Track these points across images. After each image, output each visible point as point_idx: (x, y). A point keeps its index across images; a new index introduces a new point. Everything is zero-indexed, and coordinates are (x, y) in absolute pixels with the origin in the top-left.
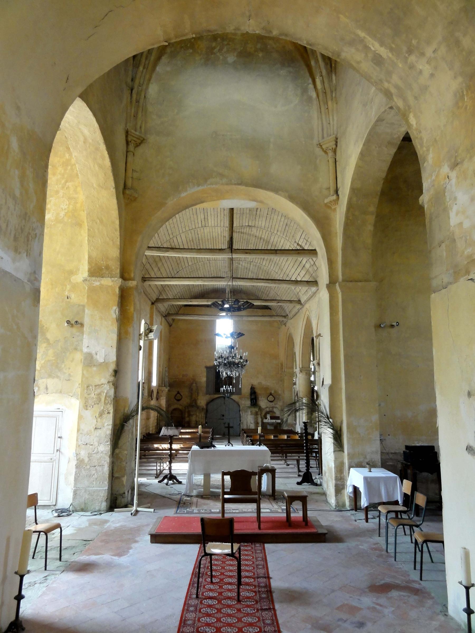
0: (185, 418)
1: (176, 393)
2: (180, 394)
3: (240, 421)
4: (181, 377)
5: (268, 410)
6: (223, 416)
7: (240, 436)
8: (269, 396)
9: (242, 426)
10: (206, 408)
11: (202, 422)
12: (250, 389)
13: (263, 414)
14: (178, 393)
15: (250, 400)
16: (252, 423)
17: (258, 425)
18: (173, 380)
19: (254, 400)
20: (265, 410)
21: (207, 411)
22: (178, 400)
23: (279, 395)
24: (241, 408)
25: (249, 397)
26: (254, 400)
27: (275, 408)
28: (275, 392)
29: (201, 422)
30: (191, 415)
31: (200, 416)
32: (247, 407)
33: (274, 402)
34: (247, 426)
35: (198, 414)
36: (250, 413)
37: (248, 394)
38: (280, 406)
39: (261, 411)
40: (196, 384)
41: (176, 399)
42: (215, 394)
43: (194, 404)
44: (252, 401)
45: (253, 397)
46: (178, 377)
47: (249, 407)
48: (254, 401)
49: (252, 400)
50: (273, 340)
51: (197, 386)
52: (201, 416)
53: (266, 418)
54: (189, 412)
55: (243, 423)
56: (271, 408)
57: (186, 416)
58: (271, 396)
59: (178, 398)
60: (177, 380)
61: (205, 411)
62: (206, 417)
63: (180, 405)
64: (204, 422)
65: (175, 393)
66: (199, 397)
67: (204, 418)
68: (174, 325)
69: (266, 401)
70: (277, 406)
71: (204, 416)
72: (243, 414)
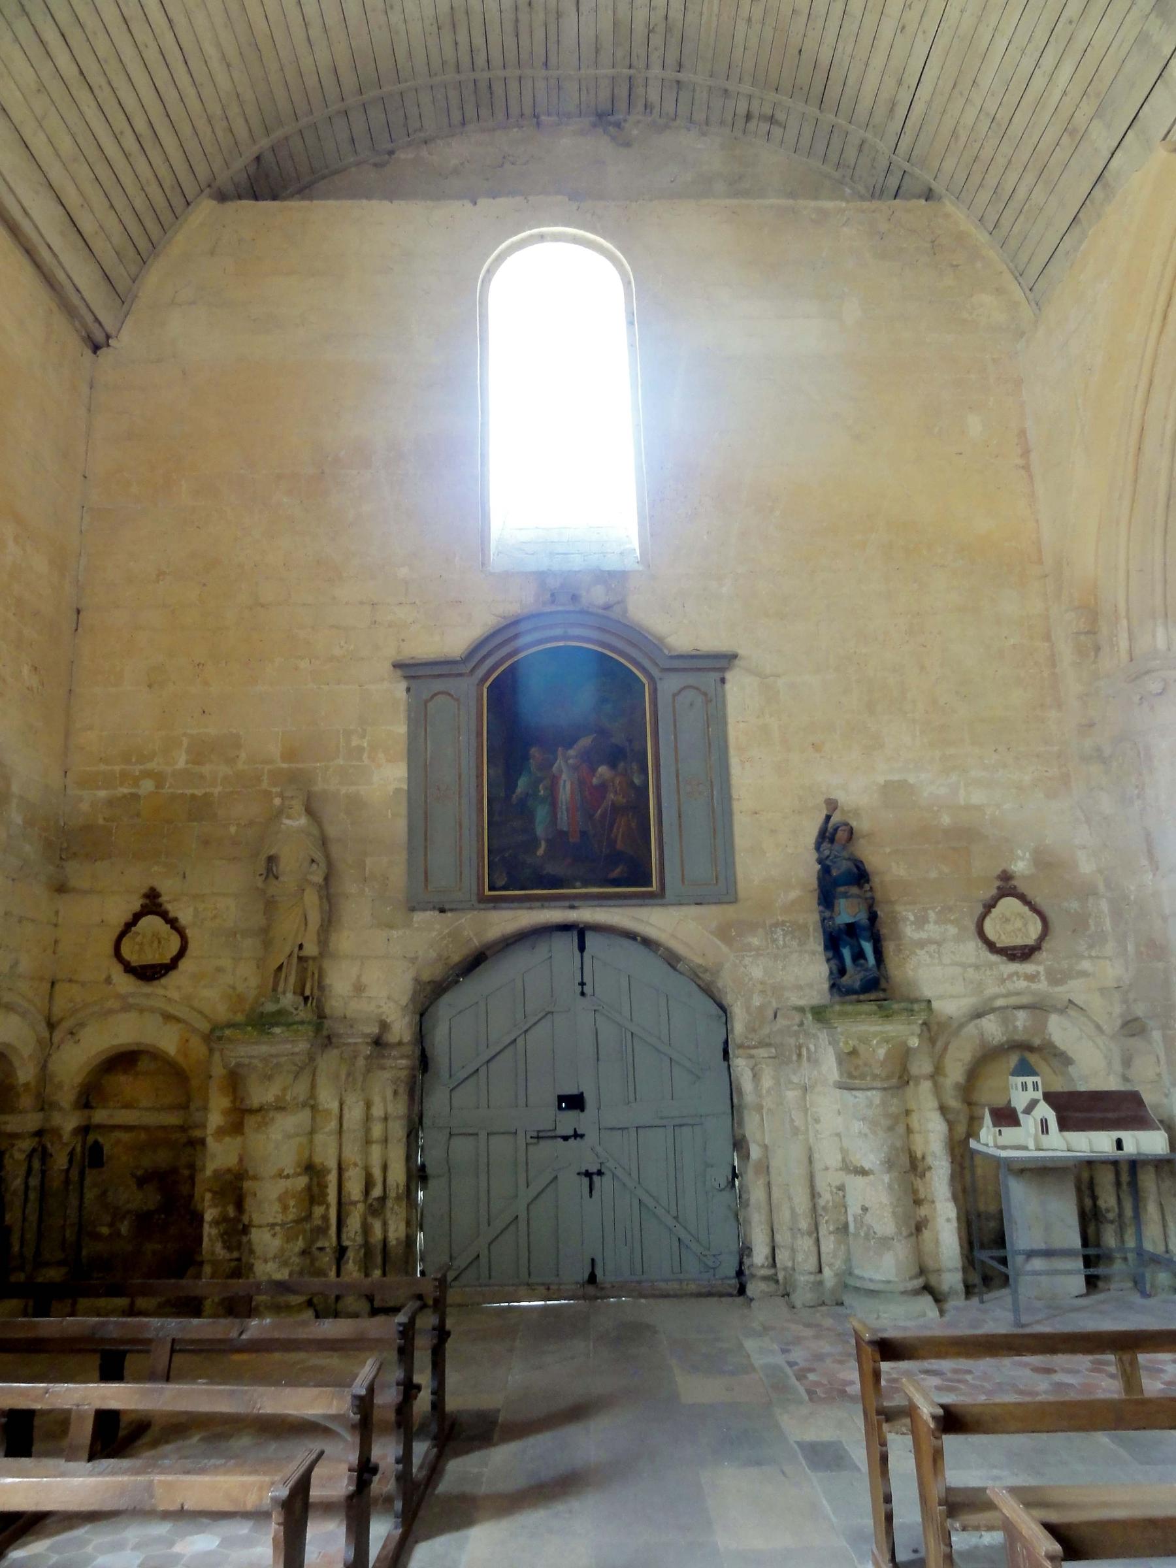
0: (202, 1142)
1: (136, 905)
2: (164, 915)
3: (739, 1144)
4: (181, 761)
5: (992, 1029)
6: (575, 1102)
7: (742, 1291)
8: (989, 906)
9: (757, 1194)
10: (407, 1038)
11: (377, 1173)
12: (818, 847)
13: (955, 1073)
14: (152, 904)
15: (816, 944)
16: (863, 1172)
17: (918, 1183)
18: (102, 794)
19: (868, 947)
20: (971, 1029)
21: (424, 1062)
22: (149, 973)
23: (1087, 892)
24: (738, 1027)
25: (811, 917)
26: (868, 947)
27: (1062, 1011)
28: (1045, 862)
29: (368, 1185)
30: (251, 1111)
31: (355, 1114)
32: (801, 1010)
33: (1043, 955)
34: (814, 1195)
35: (327, 1099)
36: (830, 1067)
37: (794, 894)
38: (1103, 991)
39: (933, 1041)
40: (310, 811)
41: (129, 969)
42: (495, 902)
43: (288, 999)
44: (846, 953)
45: (848, 912)
46: (151, 766)
47: (819, 1013)
48: (859, 955)
49: (834, 941)
50: (975, 425)
51: (324, 842)
52: (368, 1118)
53: (1006, 1117)
54: (235, 1081)
55: (765, 1168)
56: (1022, 1019)
57: (215, 1119)
58: (1009, 905)
59: (151, 957)
60: (147, 786)
61: (400, 1064)
62: (415, 1126)
63: (168, 1017)
64: (398, 1175)
65: (119, 909)
66: (345, 941)
67: (398, 1130)
68: (126, 341)
69: (972, 949)
70: (1074, 989)
71: (399, 1108)
72: (767, 1082)
